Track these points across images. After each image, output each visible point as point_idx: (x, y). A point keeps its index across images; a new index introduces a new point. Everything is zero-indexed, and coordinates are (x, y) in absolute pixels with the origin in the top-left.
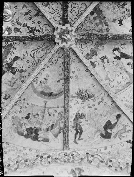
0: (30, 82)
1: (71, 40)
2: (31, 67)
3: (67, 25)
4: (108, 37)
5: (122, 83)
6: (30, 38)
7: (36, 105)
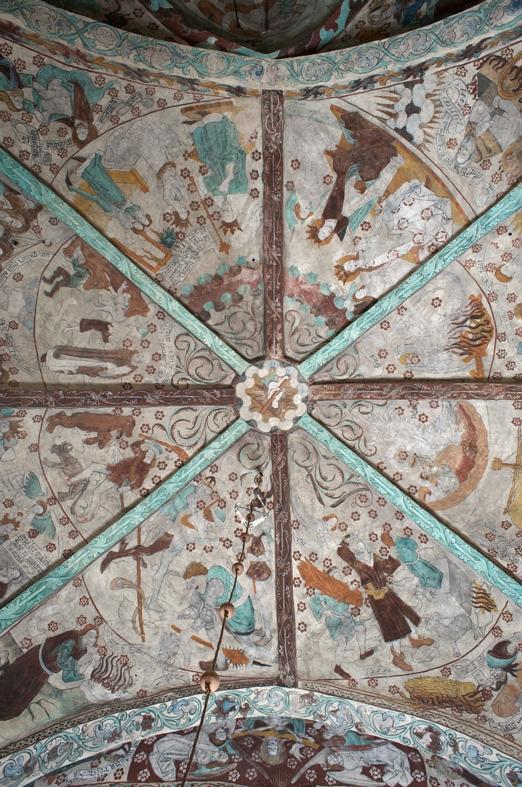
0: (427, 515)
1: (287, 377)
2: (375, 506)
3: (240, 390)
4: (274, 264)
5: (426, 204)
6: (280, 510)
7: (510, 497)
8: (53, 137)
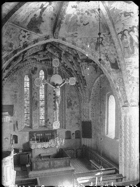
8: (106, 43)
